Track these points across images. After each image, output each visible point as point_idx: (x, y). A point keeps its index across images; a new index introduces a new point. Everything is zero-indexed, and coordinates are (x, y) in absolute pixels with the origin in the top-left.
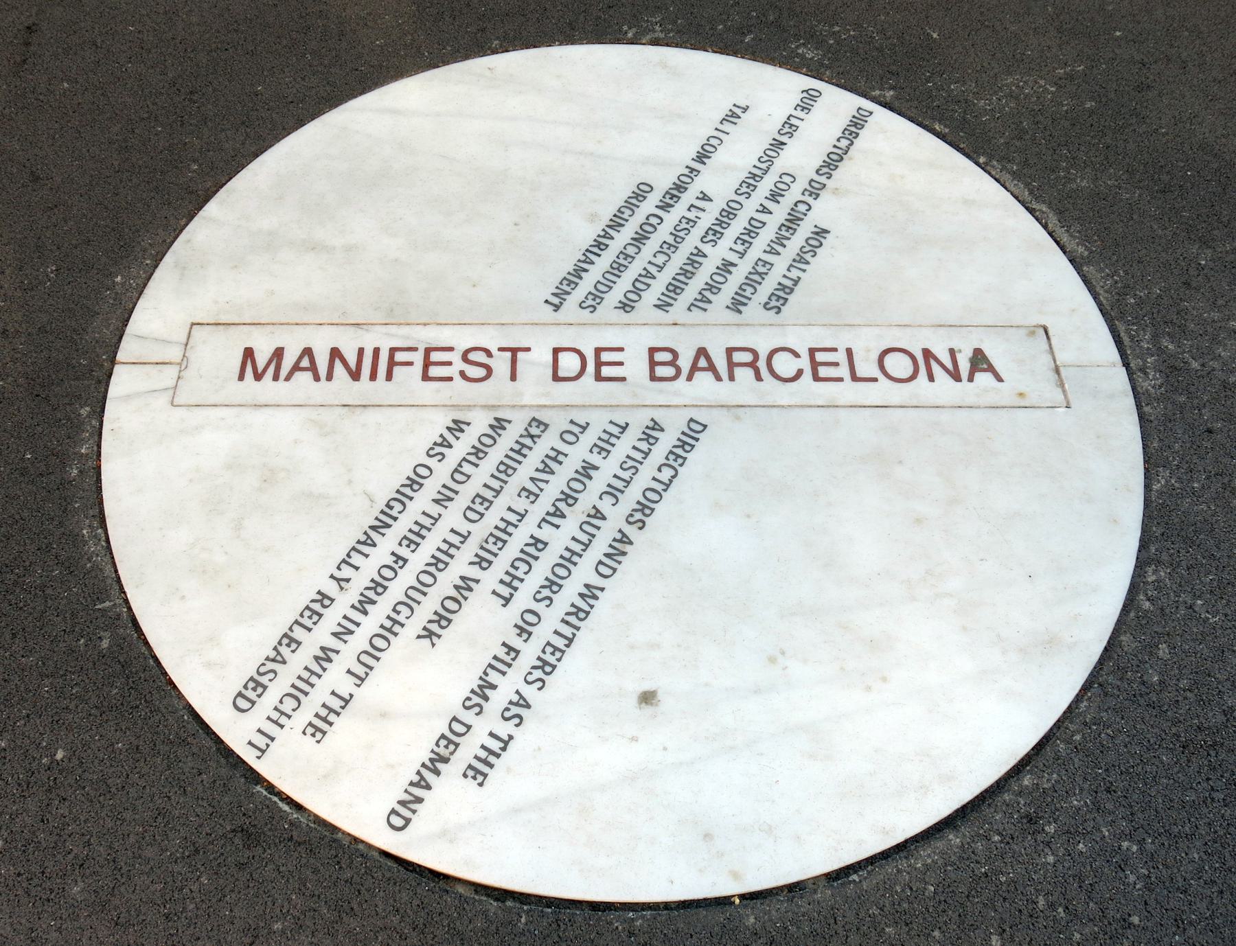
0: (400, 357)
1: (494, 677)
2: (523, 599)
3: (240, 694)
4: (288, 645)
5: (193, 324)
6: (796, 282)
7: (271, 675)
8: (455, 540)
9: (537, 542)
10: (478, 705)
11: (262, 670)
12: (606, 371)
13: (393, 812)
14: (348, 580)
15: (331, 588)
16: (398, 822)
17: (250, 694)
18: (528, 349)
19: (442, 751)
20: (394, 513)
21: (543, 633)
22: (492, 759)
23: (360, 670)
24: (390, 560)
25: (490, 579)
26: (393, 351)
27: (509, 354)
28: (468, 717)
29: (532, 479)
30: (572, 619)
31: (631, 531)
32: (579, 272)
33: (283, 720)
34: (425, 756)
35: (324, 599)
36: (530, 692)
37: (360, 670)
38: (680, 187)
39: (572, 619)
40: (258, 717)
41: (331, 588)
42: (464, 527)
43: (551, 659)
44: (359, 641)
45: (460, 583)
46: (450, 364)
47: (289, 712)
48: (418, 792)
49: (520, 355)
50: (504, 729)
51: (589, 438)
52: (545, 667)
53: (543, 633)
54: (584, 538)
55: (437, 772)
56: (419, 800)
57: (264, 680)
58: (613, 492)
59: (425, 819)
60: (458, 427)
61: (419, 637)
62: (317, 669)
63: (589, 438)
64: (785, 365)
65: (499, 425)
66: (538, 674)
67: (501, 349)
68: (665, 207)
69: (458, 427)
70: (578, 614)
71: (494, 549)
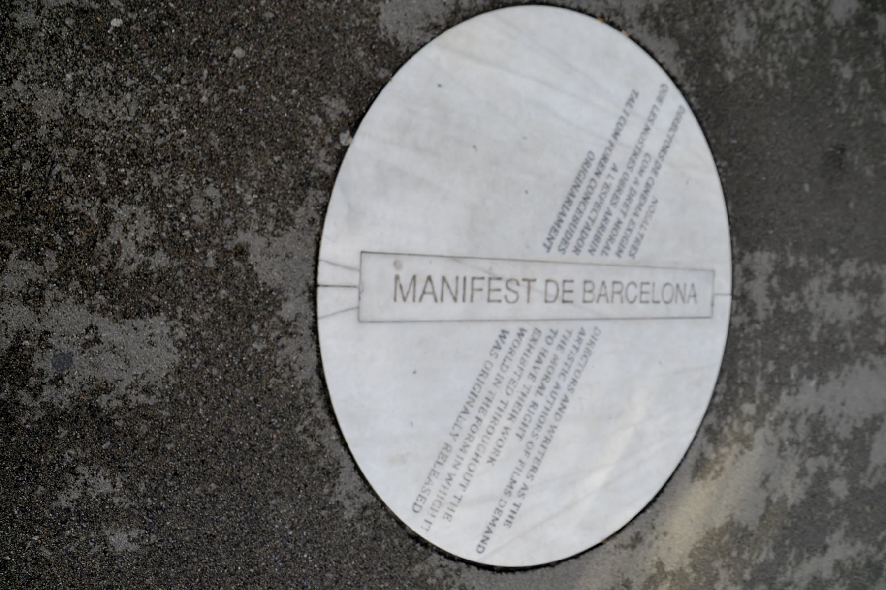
0: (478, 284)
1: (516, 478)
2: (528, 437)
3: (415, 504)
4: (434, 475)
5: (362, 252)
6: (642, 236)
7: (427, 492)
8: (502, 406)
9: (534, 405)
10: (510, 492)
11: (424, 489)
12: (567, 297)
13: (479, 546)
14: (457, 435)
15: (449, 440)
16: (481, 549)
17: (420, 503)
18: (534, 280)
19: (497, 516)
20: (476, 393)
21: (534, 453)
22: (514, 515)
23: (464, 482)
24: (475, 421)
25: (515, 426)
26: (473, 279)
27: (526, 283)
28: (506, 498)
29: (534, 368)
30: (545, 445)
31: (568, 394)
32: (560, 221)
33: (435, 513)
34: (490, 519)
35: (447, 447)
36: (529, 483)
37: (464, 482)
38: (605, 158)
39: (545, 445)
40: (425, 515)
41: (449, 440)
42: (505, 398)
43: (536, 465)
44: (463, 469)
45: (504, 431)
46: (499, 290)
47: (436, 509)
48: (487, 535)
49: (532, 284)
50: (518, 501)
51: (557, 341)
52: (534, 469)
53: (534, 453)
54: (551, 400)
55: (494, 525)
56: (488, 539)
57: (424, 495)
58: (563, 373)
59: (490, 546)
60: (503, 335)
61: (488, 462)
62: (446, 485)
63: (557, 341)
64: (633, 292)
65: (521, 334)
66: (531, 473)
67: (524, 280)
68: (598, 173)
69: (503, 335)
70: (547, 440)
71: (517, 409)
